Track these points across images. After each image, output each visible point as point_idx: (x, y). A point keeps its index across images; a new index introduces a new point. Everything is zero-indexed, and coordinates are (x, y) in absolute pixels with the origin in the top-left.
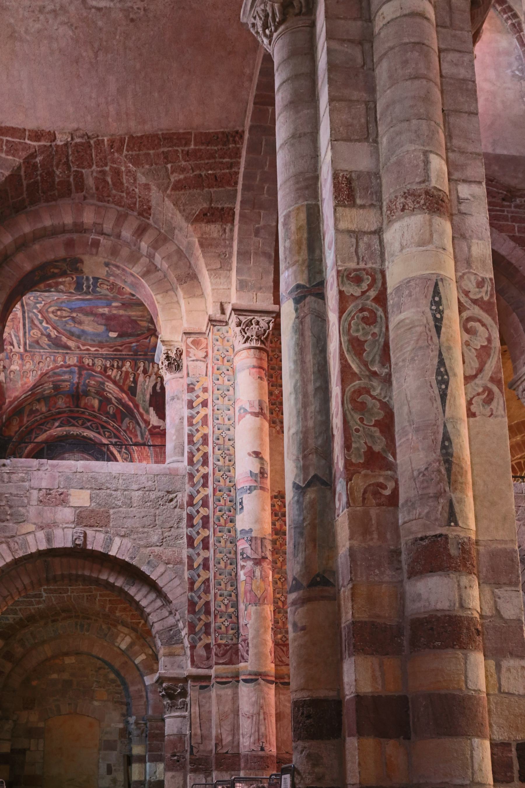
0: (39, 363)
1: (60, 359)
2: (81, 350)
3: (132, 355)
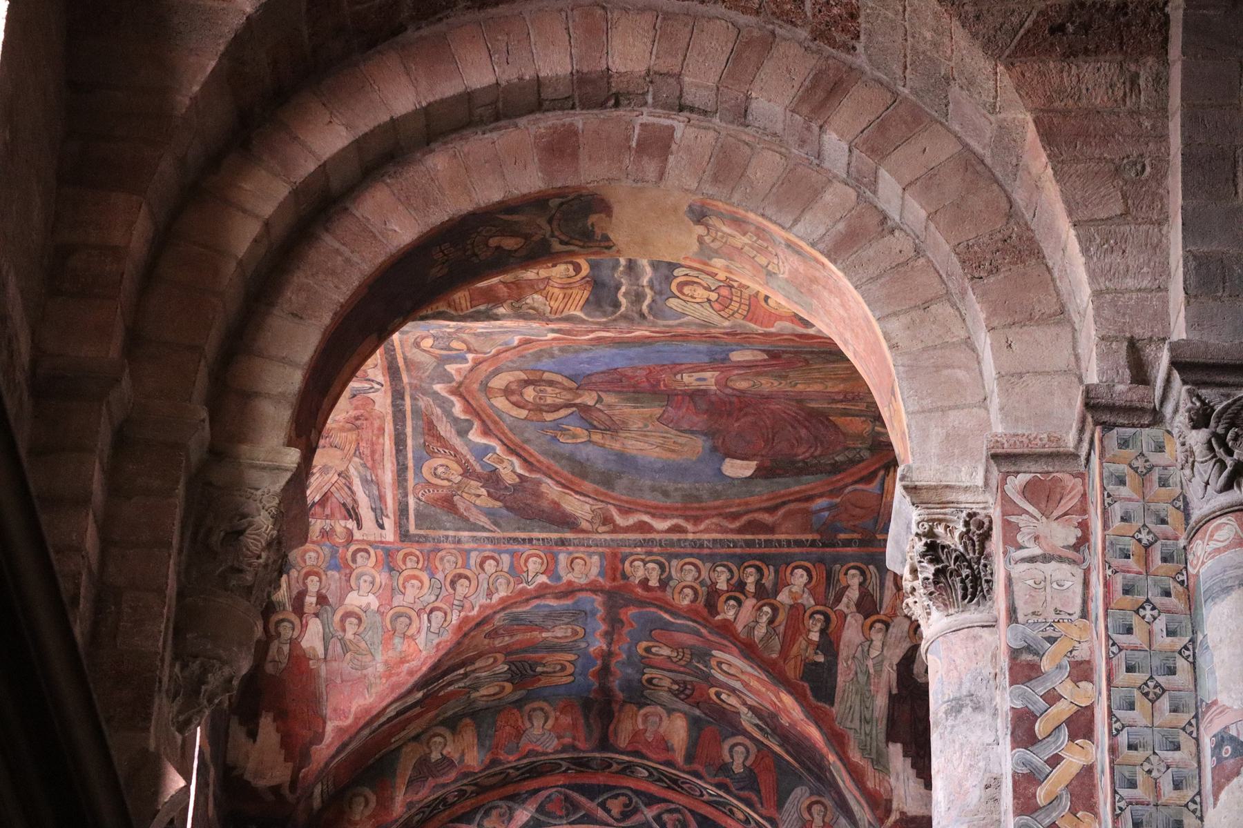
0: (453, 583)
1: (534, 565)
2: (616, 529)
3: (813, 544)
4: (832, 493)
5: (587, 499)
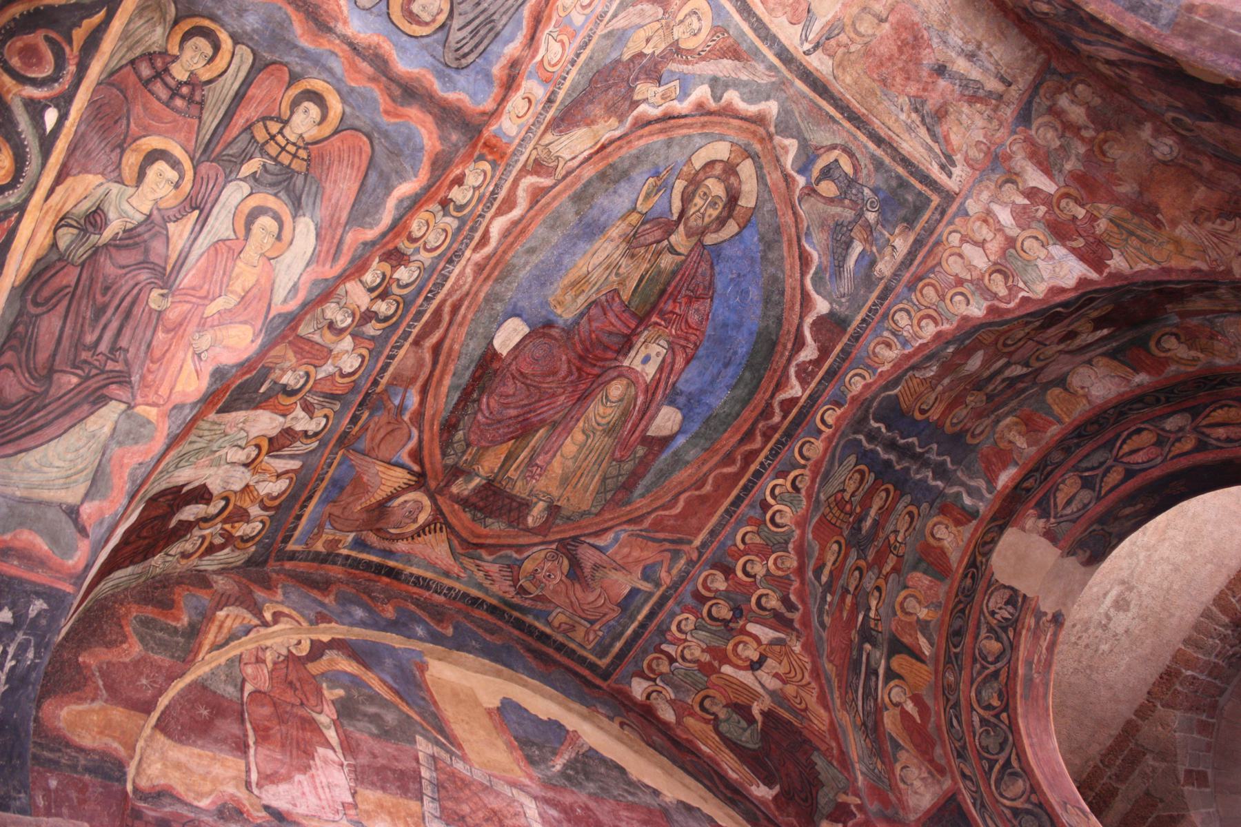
2: (524, 171)
3: (375, 383)
4: (419, 416)
5: (576, 163)
